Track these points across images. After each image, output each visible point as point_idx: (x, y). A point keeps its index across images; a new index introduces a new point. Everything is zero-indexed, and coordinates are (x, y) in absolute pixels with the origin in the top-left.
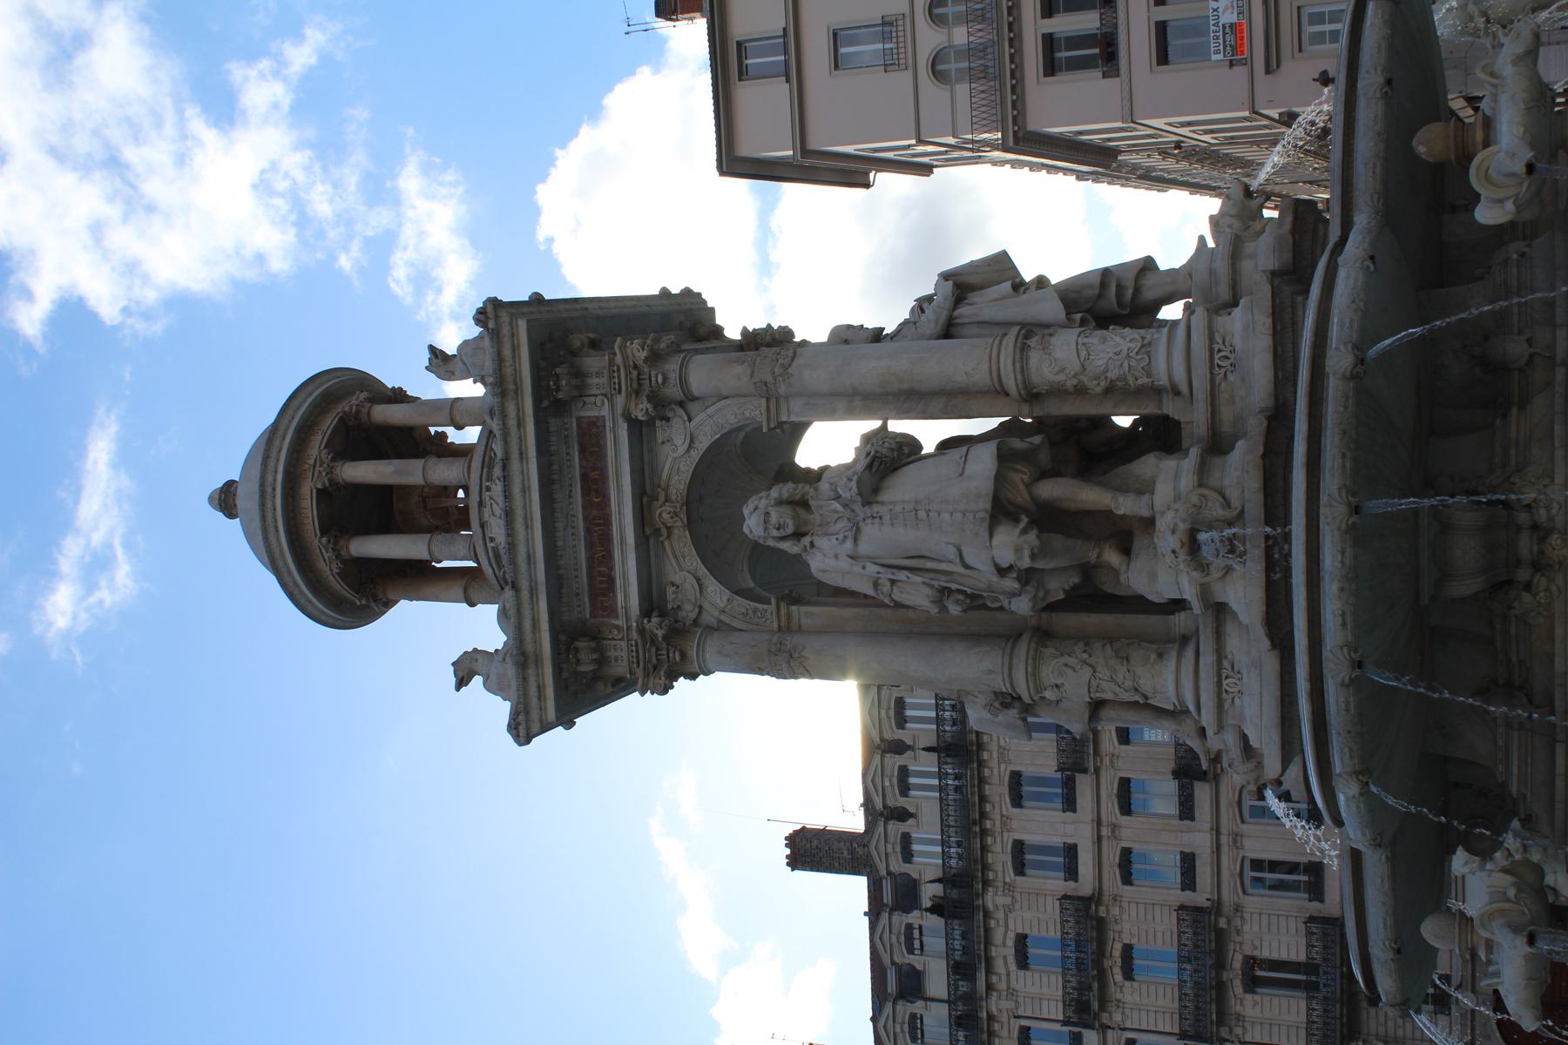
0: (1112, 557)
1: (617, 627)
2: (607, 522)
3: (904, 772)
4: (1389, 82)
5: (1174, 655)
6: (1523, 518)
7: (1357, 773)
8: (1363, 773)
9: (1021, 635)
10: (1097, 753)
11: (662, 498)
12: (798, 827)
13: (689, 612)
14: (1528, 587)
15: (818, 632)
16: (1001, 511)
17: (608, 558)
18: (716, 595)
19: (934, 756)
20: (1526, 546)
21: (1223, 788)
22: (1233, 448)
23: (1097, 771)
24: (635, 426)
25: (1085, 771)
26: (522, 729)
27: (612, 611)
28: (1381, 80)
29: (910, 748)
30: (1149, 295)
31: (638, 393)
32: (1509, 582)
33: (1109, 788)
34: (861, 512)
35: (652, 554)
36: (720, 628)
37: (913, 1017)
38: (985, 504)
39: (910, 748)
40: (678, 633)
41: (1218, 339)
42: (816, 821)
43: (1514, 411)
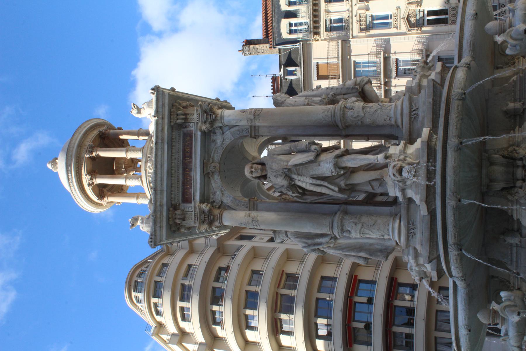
1: (191, 207)
4: (476, 14)
5: (392, 220)
6: (519, 163)
7: (457, 244)
8: (459, 247)
9: (336, 213)
11: (211, 161)
14: (521, 188)
22: (416, 141)
24: (204, 133)
26: (153, 243)
28: (474, 12)
31: (205, 122)
32: (514, 187)
35: (206, 144)
41: (413, 105)
43: (517, 127)
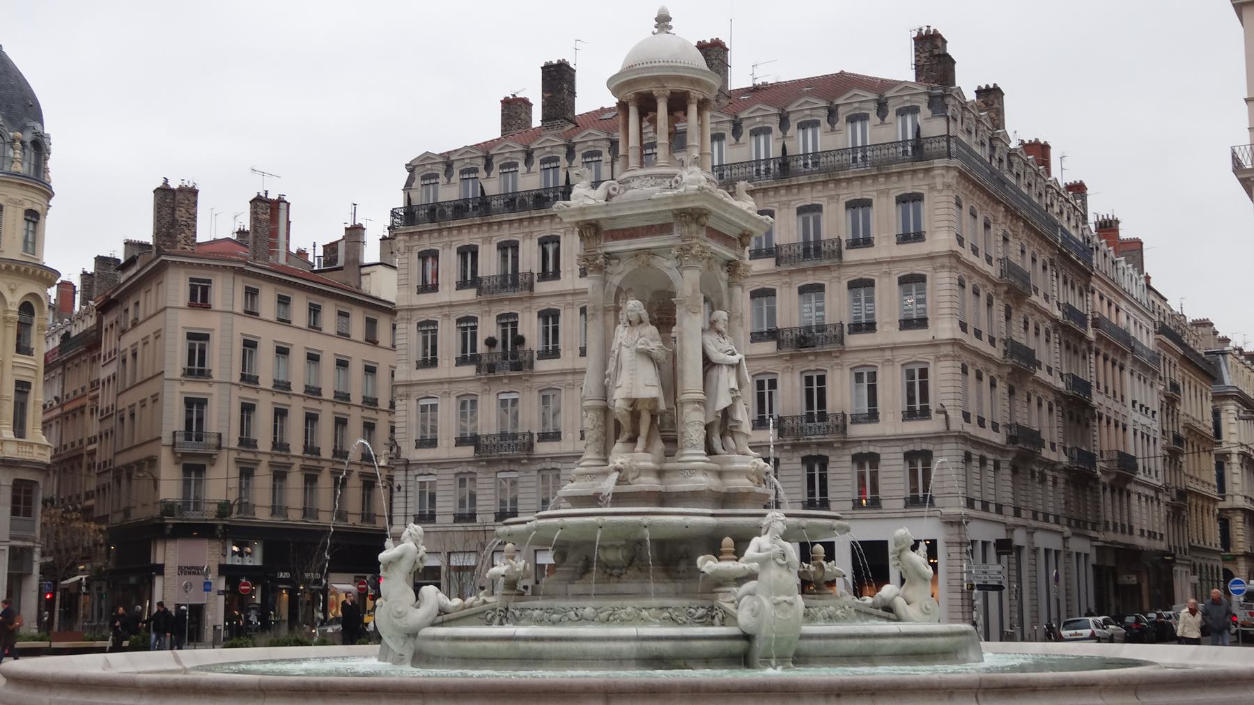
0: (626, 435)
2: (637, 236)
3: (767, 131)
10: (790, 272)
12: (728, 46)
13: (609, 269)
15: (604, 322)
16: (633, 402)
17: (625, 237)
18: (616, 280)
19: (780, 154)
20: (616, 572)
21: (773, 362)
23: (778, 273)
25: (777, 264)
27: (606, 240)
29: (784, 136)
30: (736, 437)
33: (768, 283)
34: (633, 348)
36: (605, 282)
37: (599, 154)
38: (634, 396)
39: (785, 133)
40: (599, 269)
42: (734, 59)
